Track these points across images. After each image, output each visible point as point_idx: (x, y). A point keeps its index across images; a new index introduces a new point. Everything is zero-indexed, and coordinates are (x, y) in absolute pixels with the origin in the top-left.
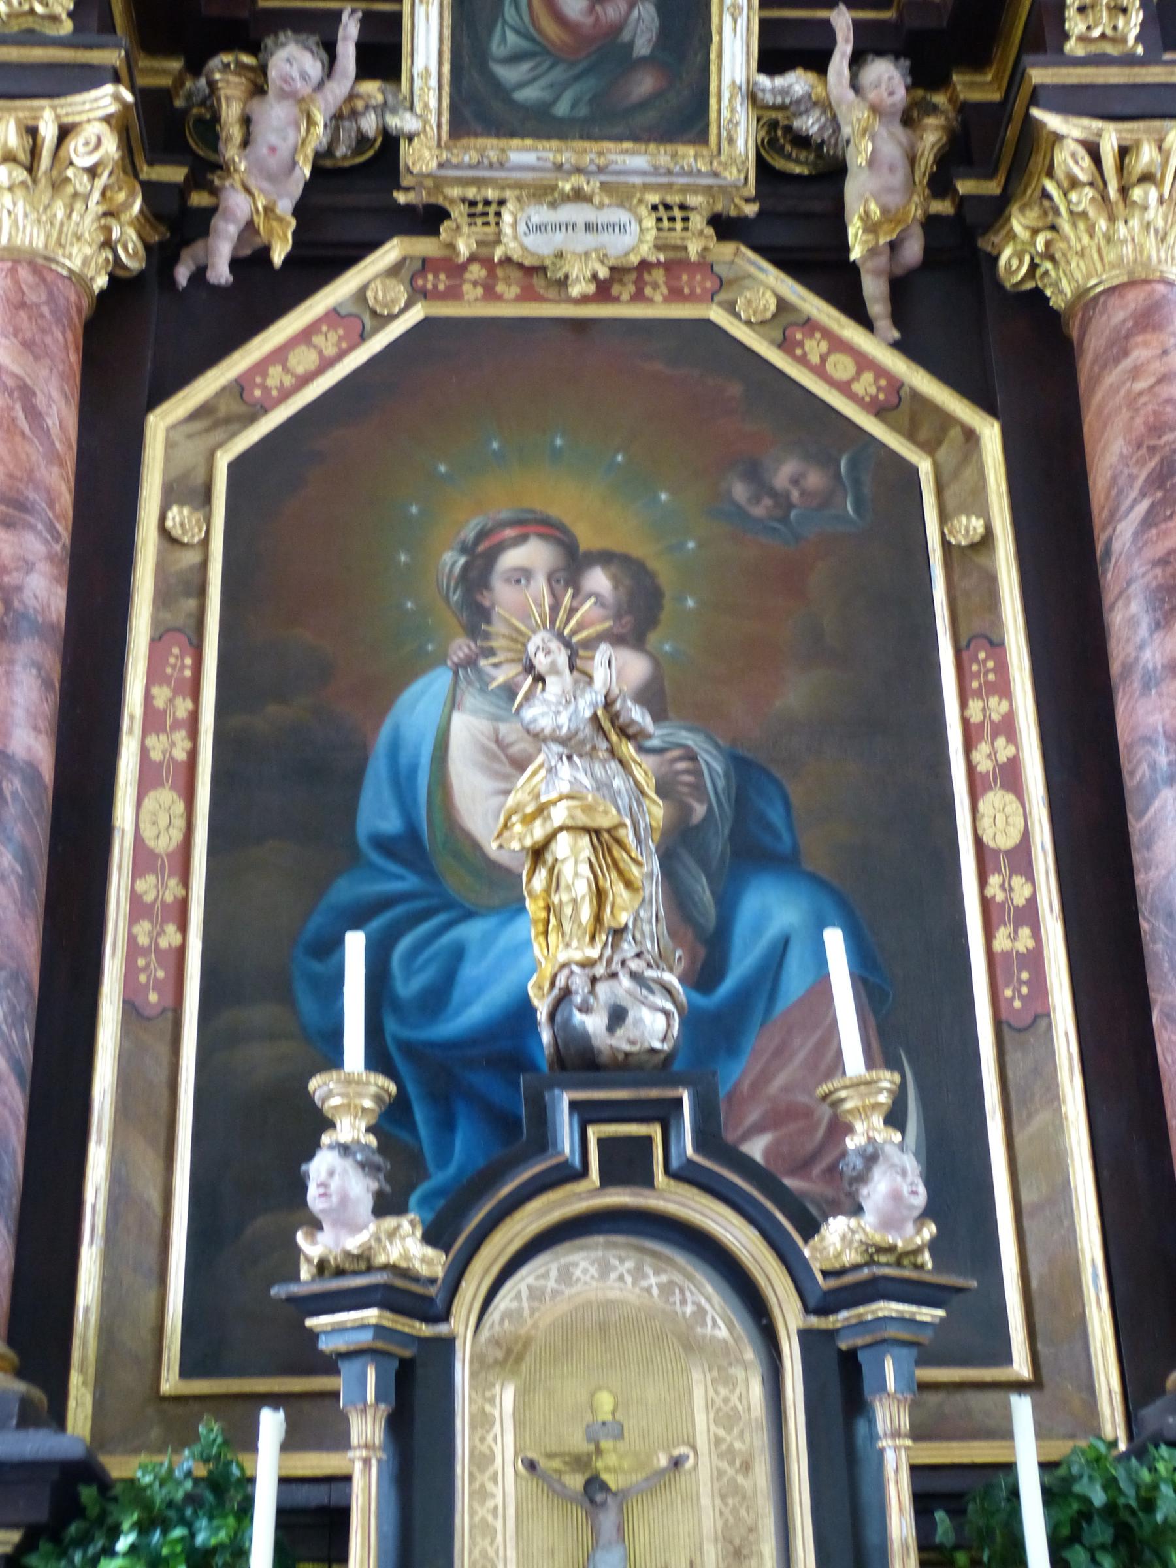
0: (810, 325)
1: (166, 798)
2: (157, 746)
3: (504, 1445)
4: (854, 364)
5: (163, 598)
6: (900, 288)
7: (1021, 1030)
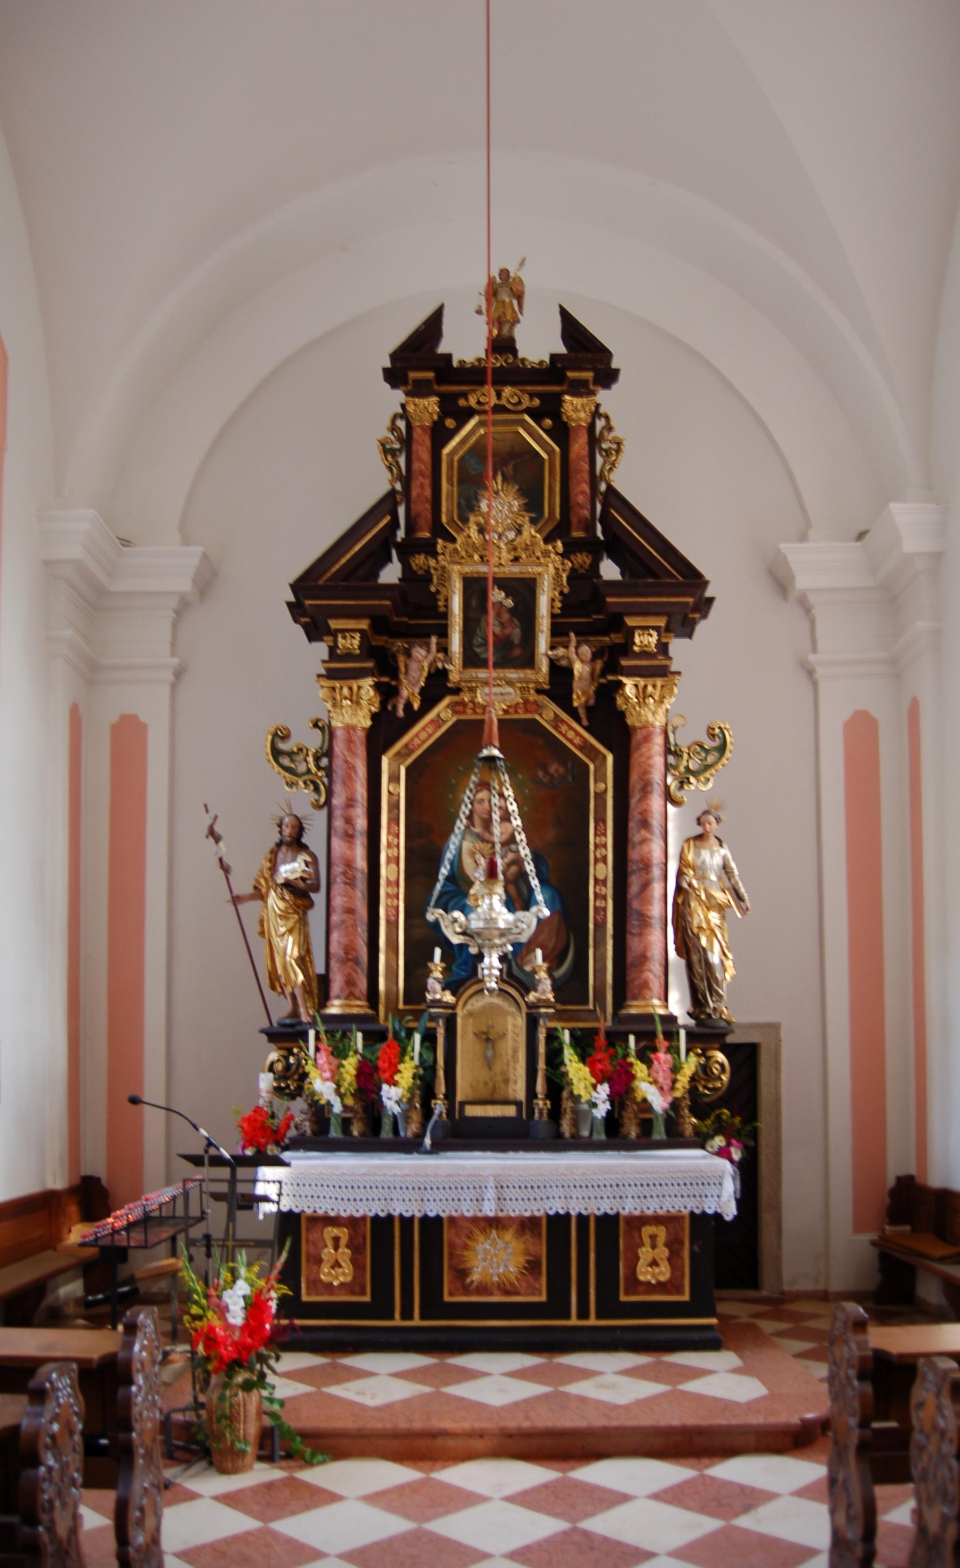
0: (563, 721)
1: (393, 866)
2: (390, 852)
3: (470, 1030)
4: (574, 734)
5: (390, 811)
6: (588, 709)
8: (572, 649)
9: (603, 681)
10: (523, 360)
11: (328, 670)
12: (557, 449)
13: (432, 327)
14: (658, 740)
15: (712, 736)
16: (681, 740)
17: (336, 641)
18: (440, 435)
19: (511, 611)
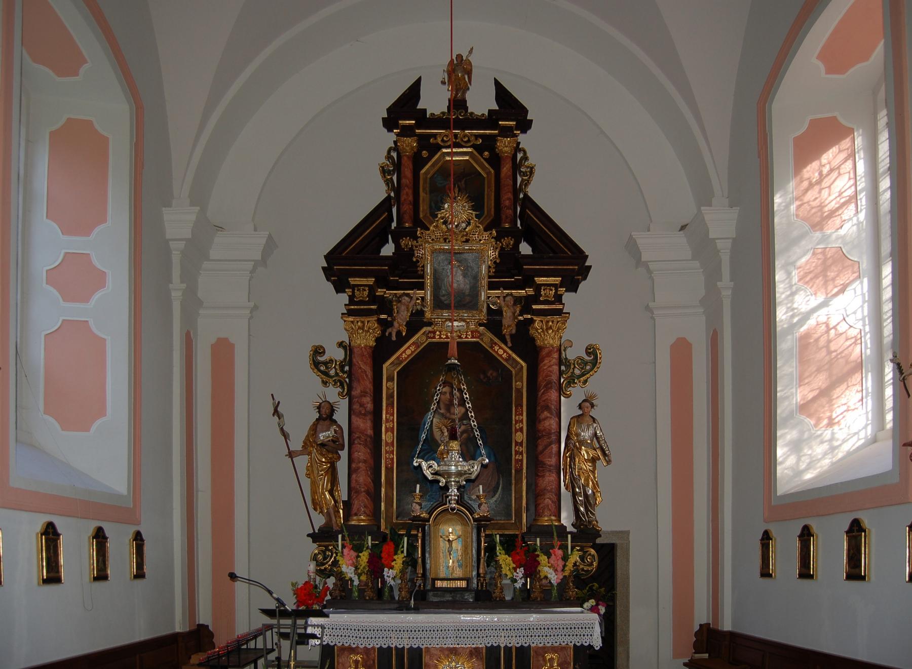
0: (496, 344)
1: (389, 433)
4: (502, 351)
5: (387, 399)
6: (512, 336)
7: (519, 471)
9: (521, 318)
10: (472, 113)
11: (348, 310)
12: (493, 171)
13: (414, 92)
14: (556, 355)
15: (588, 354)
16: (571, 354)
17: (353, 292)
18: (418, 162)
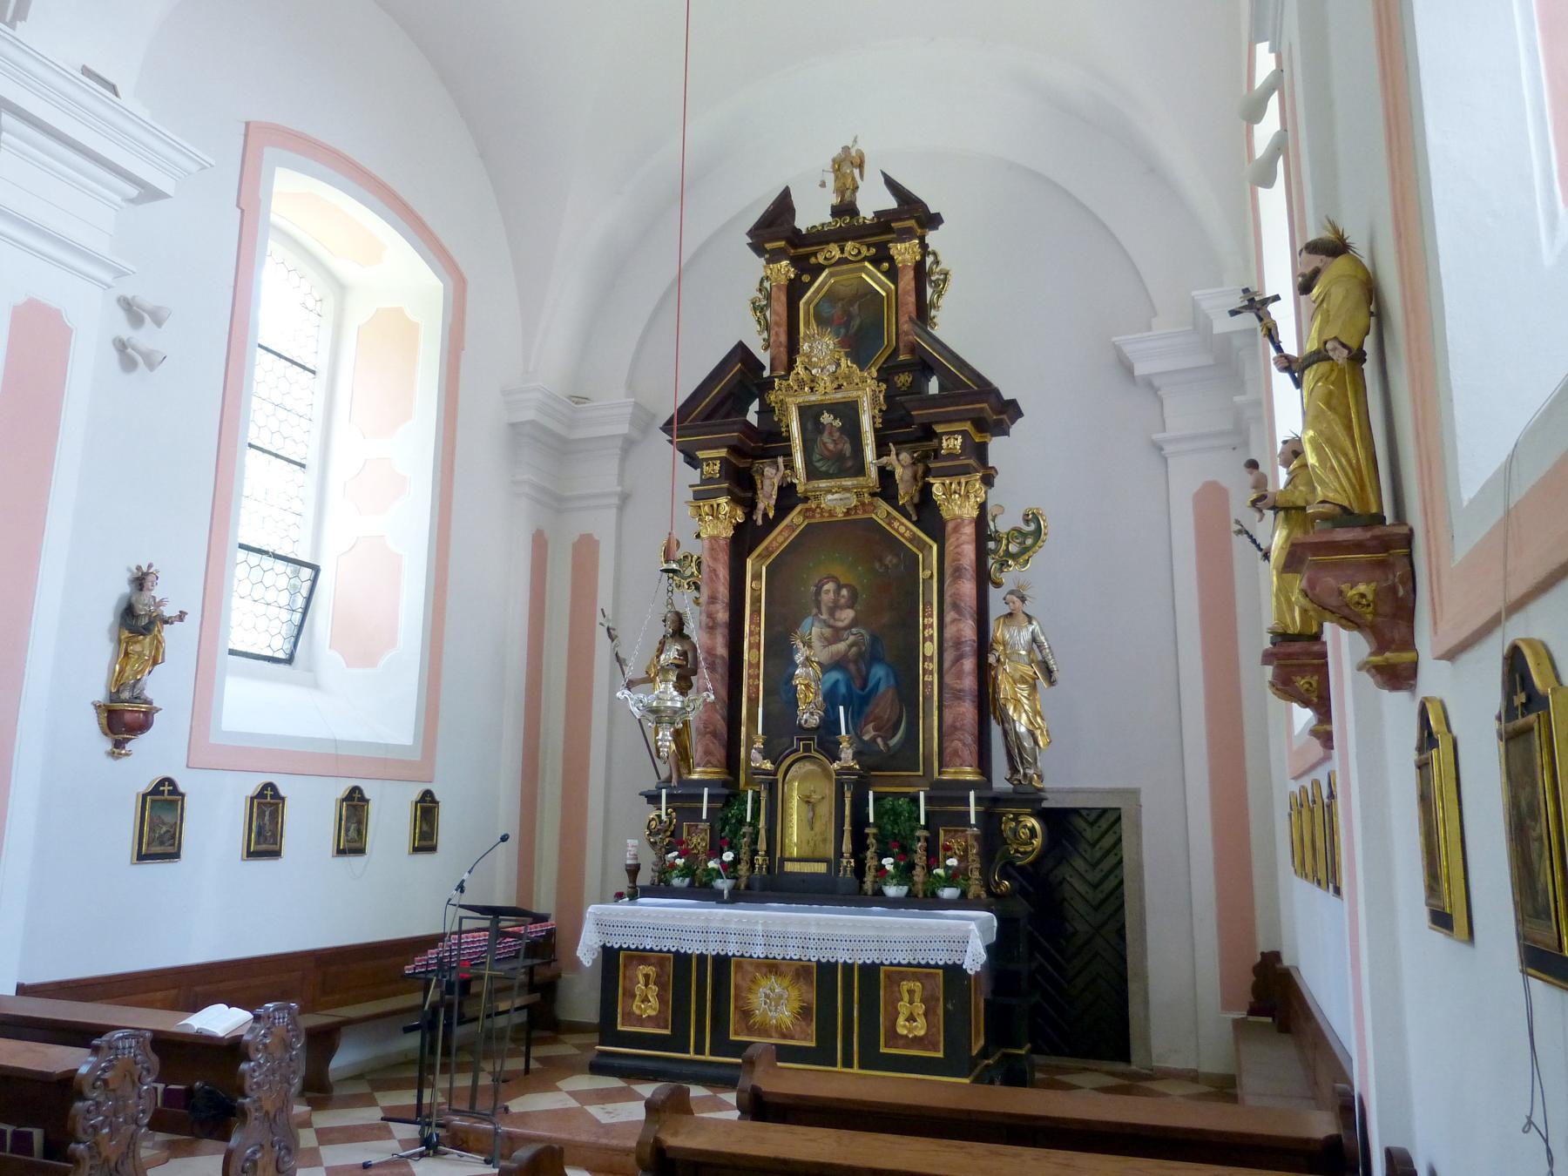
4: (904, 528)
5: (752, 604)
8: (893, 456)
15: (1027, 522)
18: (795, 290)
19: (841, 429)
